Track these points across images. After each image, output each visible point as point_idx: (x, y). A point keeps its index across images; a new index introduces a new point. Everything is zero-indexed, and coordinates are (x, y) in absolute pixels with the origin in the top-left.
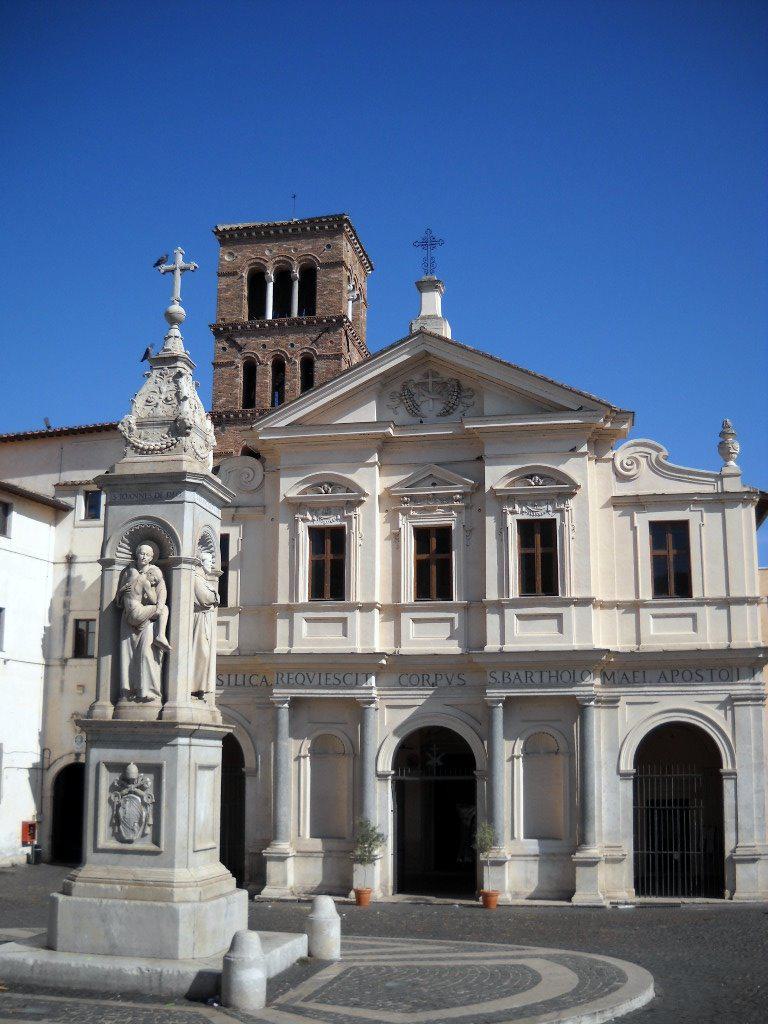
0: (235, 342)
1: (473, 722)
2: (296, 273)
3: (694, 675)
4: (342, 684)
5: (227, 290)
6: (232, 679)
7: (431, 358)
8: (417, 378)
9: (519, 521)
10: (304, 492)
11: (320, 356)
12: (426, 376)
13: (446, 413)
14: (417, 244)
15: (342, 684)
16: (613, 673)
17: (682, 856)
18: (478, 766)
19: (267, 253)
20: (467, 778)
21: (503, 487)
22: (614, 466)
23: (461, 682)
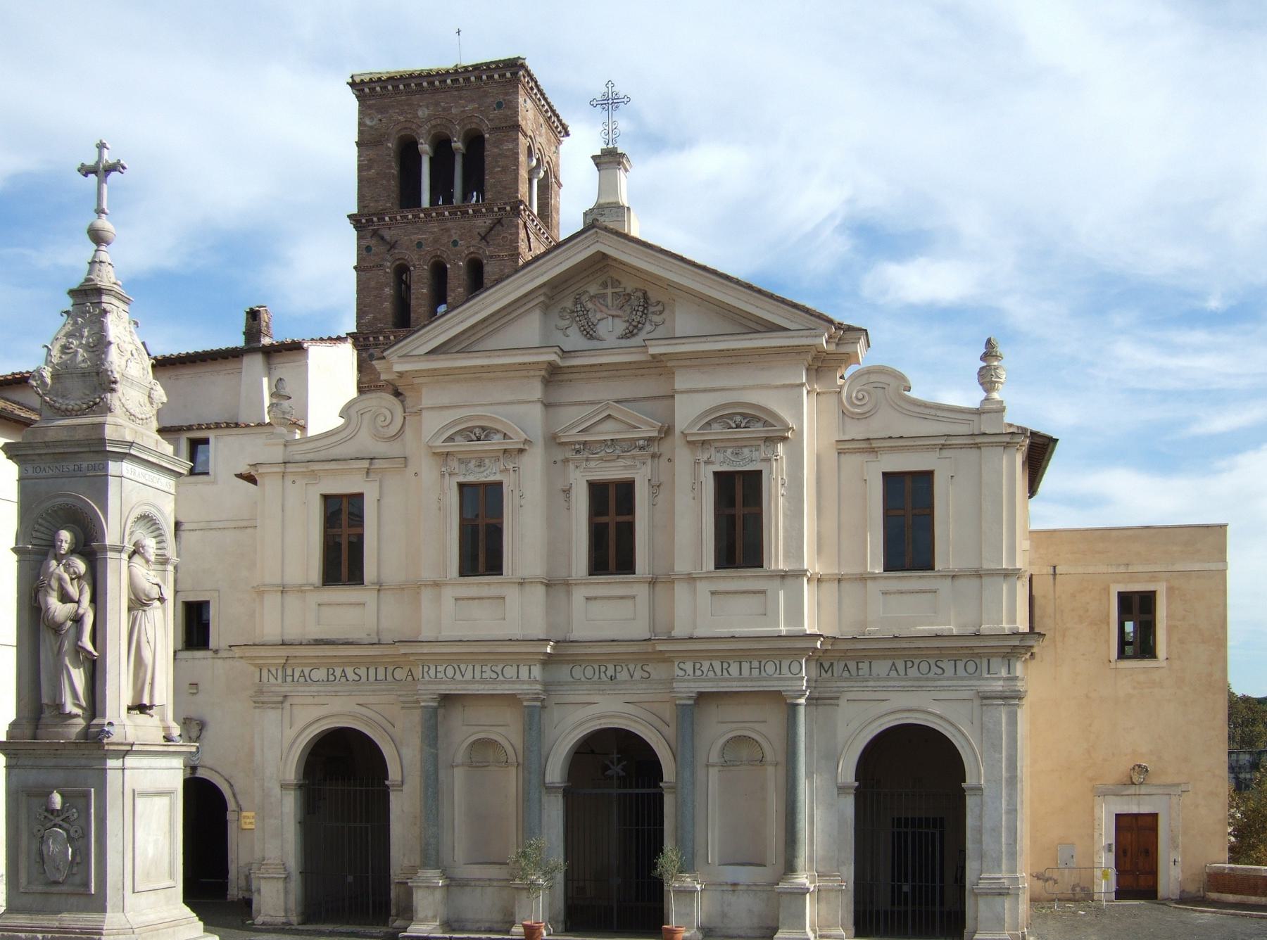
0: (382, 238)
1: (658, 723)
3: (933, 667)
4: (501, 678)
6: (372, 671)
7: (611, 263)
9: (716, 474)
11: (491, 257)
13: (629, 334)
14: (625, 100)
15: (501, 678)
16: (832, 664)
17: (913, 888)
18: (666, 778)
20: (652, 790)
21: (695, 430)
22: (840, 401)
23: (647, 675)
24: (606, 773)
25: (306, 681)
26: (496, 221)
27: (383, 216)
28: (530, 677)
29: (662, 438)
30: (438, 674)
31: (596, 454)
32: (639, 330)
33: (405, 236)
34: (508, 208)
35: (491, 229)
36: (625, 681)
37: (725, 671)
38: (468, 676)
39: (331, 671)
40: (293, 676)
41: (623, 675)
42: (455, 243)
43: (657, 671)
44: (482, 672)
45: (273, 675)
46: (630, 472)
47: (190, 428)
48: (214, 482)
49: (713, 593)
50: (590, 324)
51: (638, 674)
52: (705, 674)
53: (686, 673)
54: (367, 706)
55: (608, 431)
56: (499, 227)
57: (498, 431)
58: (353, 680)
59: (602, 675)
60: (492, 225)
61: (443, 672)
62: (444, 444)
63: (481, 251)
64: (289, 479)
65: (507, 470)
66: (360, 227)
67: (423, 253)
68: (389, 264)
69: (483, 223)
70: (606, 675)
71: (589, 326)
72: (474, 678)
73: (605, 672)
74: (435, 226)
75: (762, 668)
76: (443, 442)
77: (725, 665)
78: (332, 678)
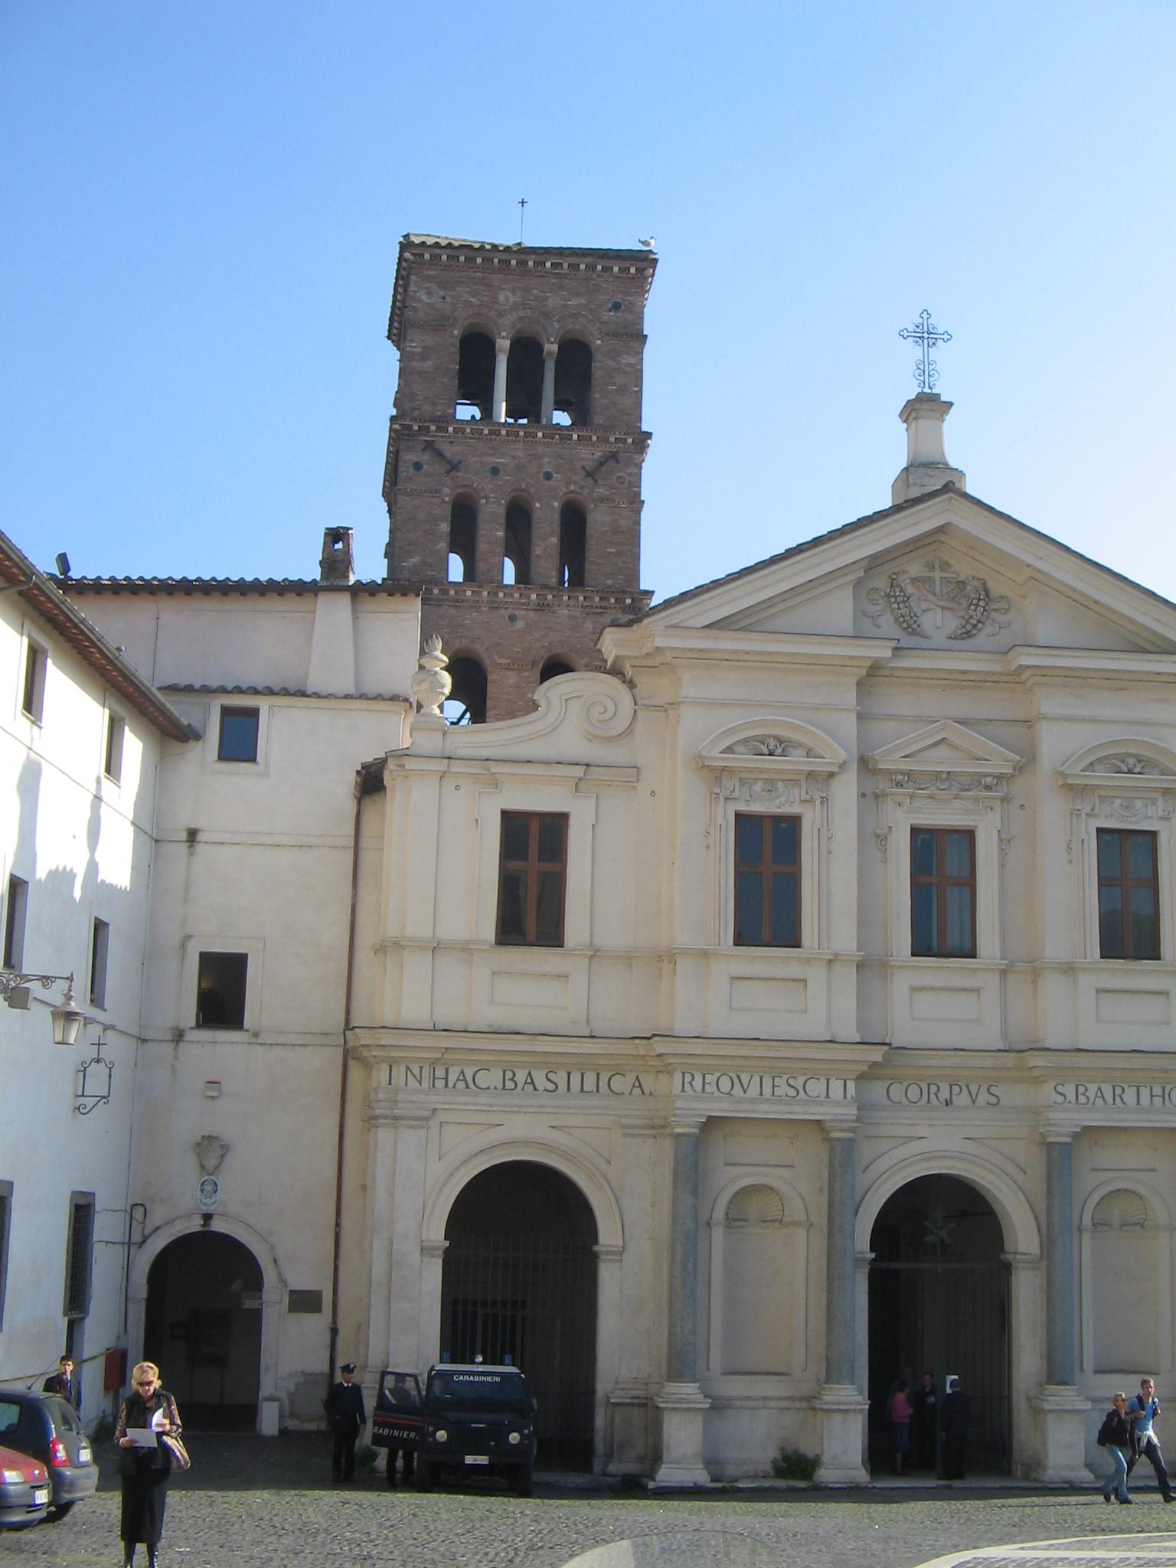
2: (551, 348)
5: (424, 357)
6: (576, 1079)
8: (915, 569)
9: (1099, 831)
10: (729, 750)
11: (602, 500)
12: (931, 567)
19: (501, 298)
21: (1077, 770)
23: (994, 1100)
24: (926, 1240)
25: (467, 1087)
26: (609, 455)
27: (445, 425)
28: (845, 1097)
29: (1012, 776)
30: (706, 1086)
31: (922, 789)
32: (979, 630)
33: (474, 456)
34: (630, 440)
35: (602, 464)
36: (966, 1107)
37: (1118, 1100)
38: (753, 1091)
39: (509, 1075)
40: (446, 1079)
41: (962, 1099)
42: (548, 476)
43: (1012, 1095)
44: (774, 1086)
45: (416, 1078)
46: (972, 818)
47: (223, 690)
48: (266, 775)
49: (1098, 991)
50: (912, 614)
51: (983, 1098)
52: (1091, 1100)
53: (1065, 1098)
54: (907, 1140)
55: (941, 761)
56: (612, 463)
57: (801, 745)
58: (546, 1090)
59: (932, 1097)
60: (603, 459)
61: (714, 1084)
62: (722, 755)
63: (586, 491)
64: (449, 784)
65: (811, 801)
66: (408, 435)
67: (500, 483)
68: (448, 491)
69: (590, 455)
70: (937, 1097)
71: (911, 617)
72: (761, 1094)
73: (936, 1094)
74: (519, 449)
75: (1167, 1096)
76: (721, 753)
77: (1118, 1091)
78: (510, 1085)
